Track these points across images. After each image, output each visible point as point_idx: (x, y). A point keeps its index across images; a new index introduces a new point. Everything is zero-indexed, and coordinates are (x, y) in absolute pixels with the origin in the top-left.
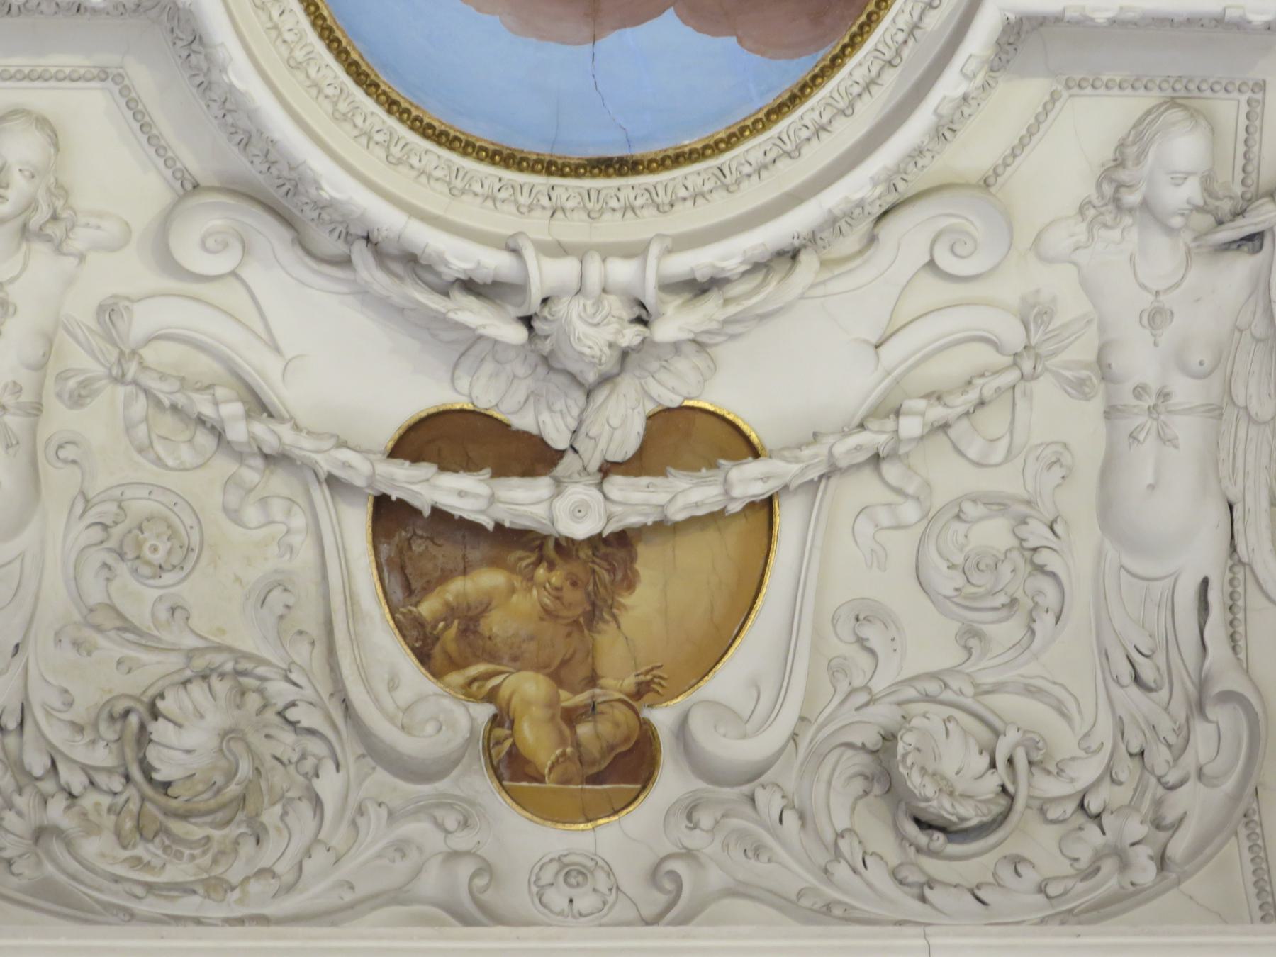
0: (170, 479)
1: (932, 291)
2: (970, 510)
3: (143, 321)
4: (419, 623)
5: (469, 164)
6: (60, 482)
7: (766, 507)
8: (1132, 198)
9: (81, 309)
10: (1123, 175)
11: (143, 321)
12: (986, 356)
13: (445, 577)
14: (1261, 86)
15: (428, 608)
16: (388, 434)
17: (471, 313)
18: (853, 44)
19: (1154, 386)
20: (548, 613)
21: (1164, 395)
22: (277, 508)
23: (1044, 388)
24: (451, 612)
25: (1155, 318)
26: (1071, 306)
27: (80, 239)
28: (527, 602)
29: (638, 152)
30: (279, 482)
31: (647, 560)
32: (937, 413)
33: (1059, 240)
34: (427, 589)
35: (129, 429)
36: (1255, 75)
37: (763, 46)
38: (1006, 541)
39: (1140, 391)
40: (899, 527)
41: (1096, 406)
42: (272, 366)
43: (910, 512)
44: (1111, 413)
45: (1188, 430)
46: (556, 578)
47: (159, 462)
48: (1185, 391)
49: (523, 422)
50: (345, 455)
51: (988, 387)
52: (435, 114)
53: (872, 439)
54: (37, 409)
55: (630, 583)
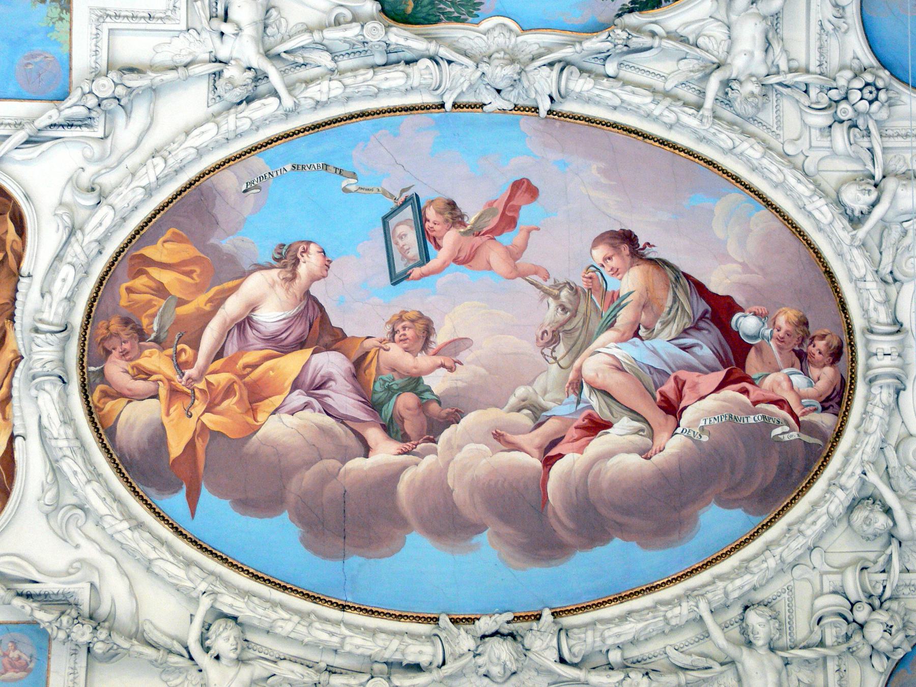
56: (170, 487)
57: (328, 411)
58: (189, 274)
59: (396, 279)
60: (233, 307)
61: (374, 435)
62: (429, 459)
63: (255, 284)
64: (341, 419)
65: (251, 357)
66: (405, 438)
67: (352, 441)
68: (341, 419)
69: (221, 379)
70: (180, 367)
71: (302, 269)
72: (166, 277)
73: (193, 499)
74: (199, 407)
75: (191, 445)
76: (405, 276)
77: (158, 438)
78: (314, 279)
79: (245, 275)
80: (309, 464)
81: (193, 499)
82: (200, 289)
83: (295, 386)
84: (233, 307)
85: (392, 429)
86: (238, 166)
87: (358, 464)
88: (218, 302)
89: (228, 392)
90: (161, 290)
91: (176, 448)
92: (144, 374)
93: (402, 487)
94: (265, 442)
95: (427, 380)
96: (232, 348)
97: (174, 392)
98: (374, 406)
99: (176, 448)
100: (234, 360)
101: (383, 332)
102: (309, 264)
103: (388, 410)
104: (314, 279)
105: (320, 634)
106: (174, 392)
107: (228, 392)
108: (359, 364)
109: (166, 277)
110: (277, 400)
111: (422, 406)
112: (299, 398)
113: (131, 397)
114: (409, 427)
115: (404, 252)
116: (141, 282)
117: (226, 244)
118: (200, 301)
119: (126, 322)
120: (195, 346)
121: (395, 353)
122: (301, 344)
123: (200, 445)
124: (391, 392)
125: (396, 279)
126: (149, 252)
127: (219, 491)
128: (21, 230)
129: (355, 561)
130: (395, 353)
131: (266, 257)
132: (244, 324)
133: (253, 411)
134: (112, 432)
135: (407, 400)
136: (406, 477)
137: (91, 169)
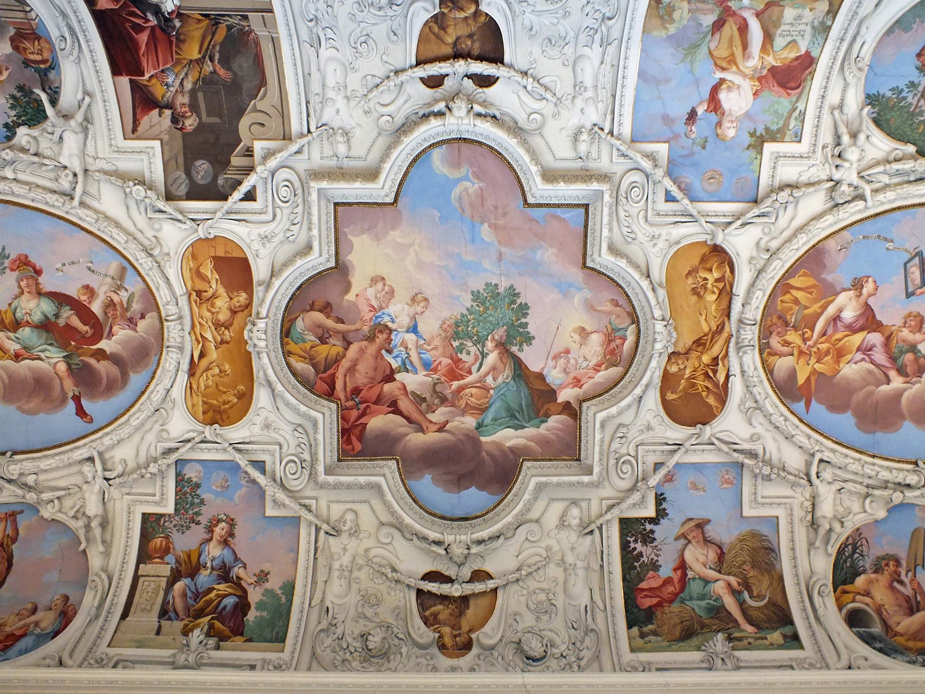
0: (377, 586)
1: (527, 545)
2: (537, 591)
3: (372, 553)
4: (425, 617)
5: (436, 519)
6: (354, 587)
7: (495, 590)
8: (566, 523)
9: (361, 550)
10: (564, 519)
11: (372, 553)
12: (539, 558)
13: (431, 607)
14: (590, 500)
15: (427, 613)
16: (420, 576)
17: (435, 548)
18: (509, 493)
19: (573, 563)
20: (451, 614)
21: (575, 565)
22: (398, 592)
23: (552, 565)
24: (432, 614)
25: (572, 549)
26: (556, 547)
27: (361, 536)
28: (447, 612)
29: (468, 516)
30: (399, 586)
31: (472, 603)
32: (529, 570)
33: (553, 534)
34: (427, 609)
35: (369, 575)
36: (588, 497)
37: (491, 494)
38: (546, 598)
39: (570, 565)
40: (523, 595)
41: (562, 569)
42: (398, 562)
43: (525, 592)
44: (565, 570)
45: (581, 572)
46: (453, 607)
47: (375, 583)
48: (580, 564)
49: (446, 573)
50: (410, 579)
51: (539, 565)
52: (430, 509)
53: (517, 575)
54: (351, 572)
55: (468, 609)
56: (796, 399)
57: (872, 362)
58: (811, 293)
59: (909, 295)
60: (831, 310)
61: (893, 374)
62: (918, 386)
63: (842, 298)
64: (878, 366)
65: (839, 335)
66: (907, 375)
67: (882, 377)
68: (878, 366)
69: (824, 346)
70: (805, 340)
71: (865, 291)
72: (799, 295)
73: (808, 405)
74: (813, 360)
75: (808, 379)
76: (913, 294)
77: (793, 374)
78: (870, 295)
79: (837, 294)
80: (861, 388)
81: (808, 405)
82: (816, 301)
83: (858, 349)
84: (831, 310)
85: (901, 371)
86: (837, 236)
87: (884, 388)
88: (824, 308)
89: (827, 353)
90: (796, 301)
91: (801, 380)
92: (787, 343)
93: (904, 400)
94: (842, 378)
95: (920, 347)
96: (830, 332)
97: (801, 353)
98: (893, 359)
99: (801, 380)
100: (831, 336)
101: (900, 322)
102: (868, 288)
103: (900, 362)
104: (870, 295)
105: (868, 470)
106: (801, 353)
107: (827, 353)
108: (888, 339)
109: (799, 295)
110: (849, 357)
111: (916, 360)
112: (859, 356)
113: (781, 355)
114: (909, 370)
115: (913, 281)
116: (787, 297)
117: (829, 278)
118: (816, 308)
119: (780, 317)
120: (812, 330)
121: (906, 334)
122: (862, 329)
123: (813, 379)
124: (902, 352)
125: (909, 295)
126: (792, 282)
127: (820, 401)
128: (732, 271)
129: (879, 434)
130: (906, 334)
131: (848, 285)
132: (836, 319)
133: (838, 362)
134: (771, 372)
135: (909, 357)
136: (906, 394)
137: (766, 238)
